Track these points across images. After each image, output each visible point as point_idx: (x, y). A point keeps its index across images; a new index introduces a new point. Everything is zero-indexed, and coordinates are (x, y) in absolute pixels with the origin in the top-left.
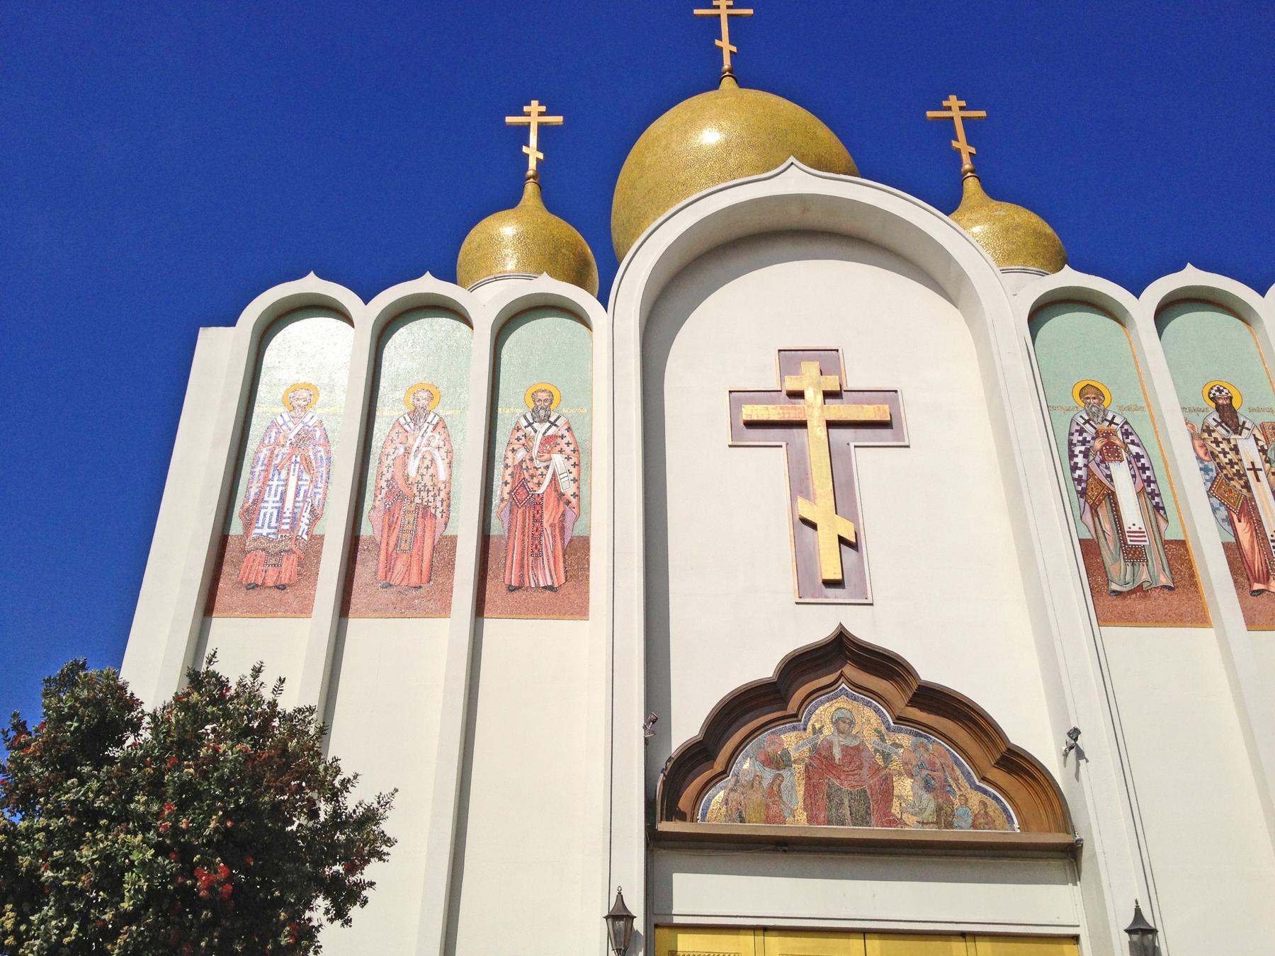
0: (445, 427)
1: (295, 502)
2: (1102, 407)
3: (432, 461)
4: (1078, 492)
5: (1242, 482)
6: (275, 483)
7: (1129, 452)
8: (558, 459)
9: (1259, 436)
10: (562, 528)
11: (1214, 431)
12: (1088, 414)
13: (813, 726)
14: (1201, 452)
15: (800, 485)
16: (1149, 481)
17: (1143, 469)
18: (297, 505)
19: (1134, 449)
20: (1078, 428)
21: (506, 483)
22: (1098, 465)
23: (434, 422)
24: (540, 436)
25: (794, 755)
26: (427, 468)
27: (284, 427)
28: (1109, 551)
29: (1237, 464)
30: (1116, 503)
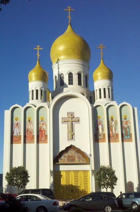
8: (44, 126)
17: (102, 126)
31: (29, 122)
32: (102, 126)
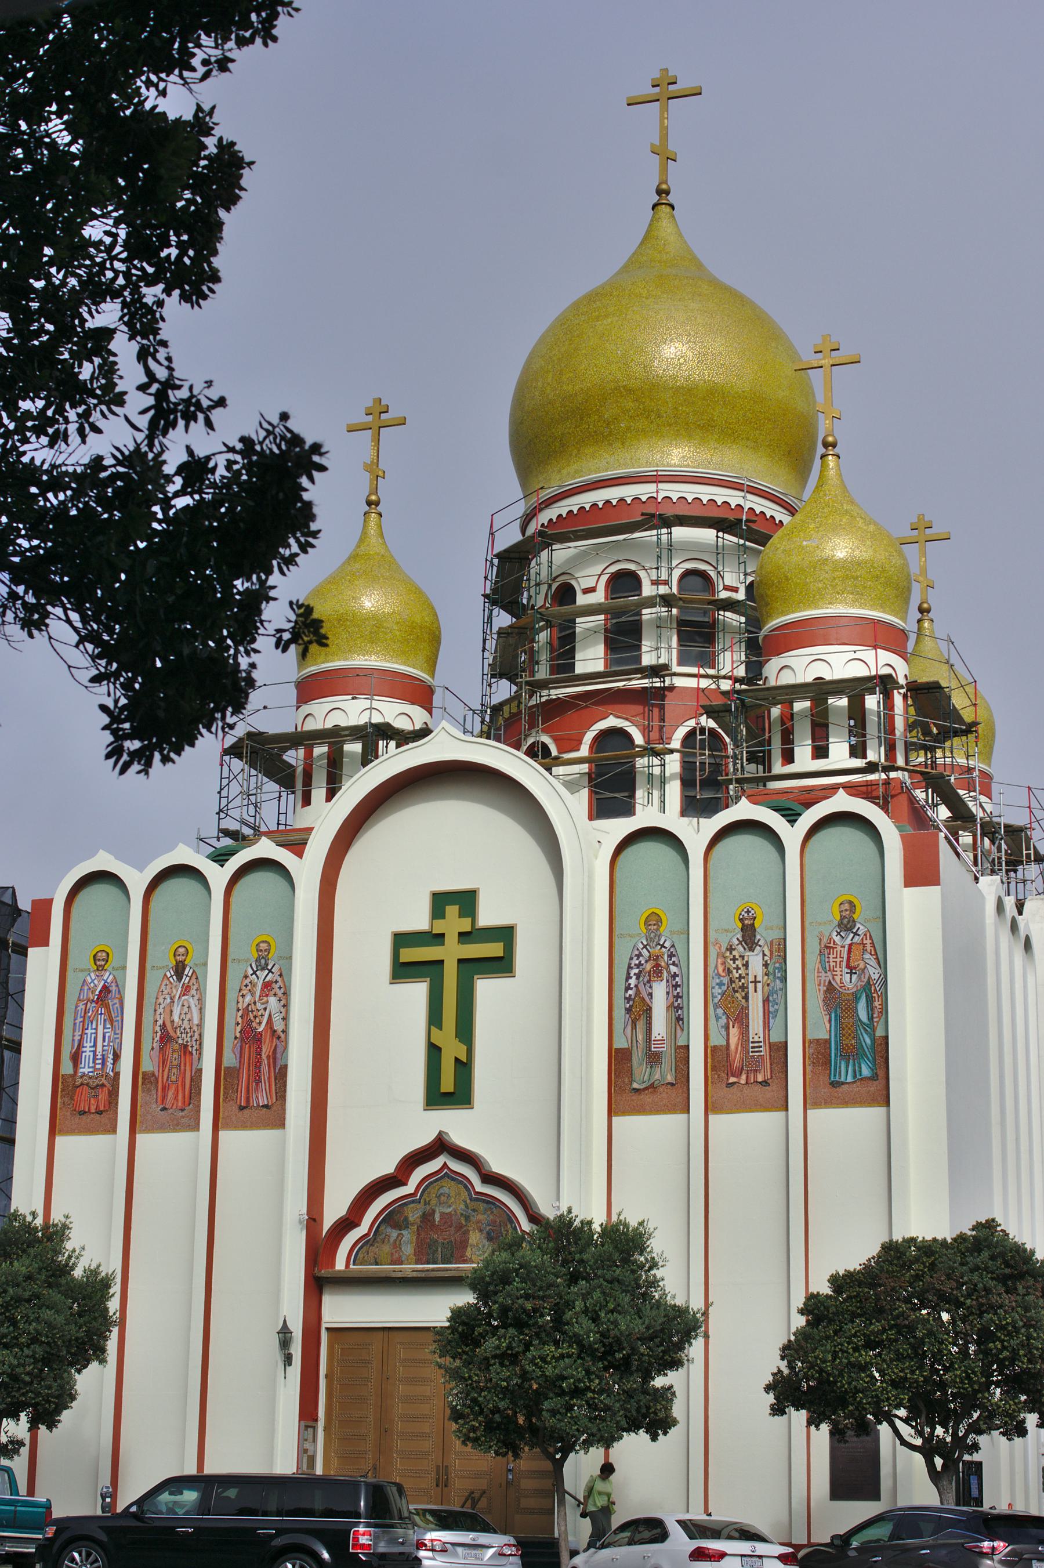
0: (197, 978)
1: (104, 1046)
2: (658, 933)
3: (189, 1007)
4: (626, 1009)
5: (743, 994)
6: (89, 1031)
7: (669, 972)
8: (272, 1000)
9: (767, 952)
10: (275, 1059)
11: (734, 949)
12: (647, 940)
13: (425, 1201)
14: (721, 969)
15: (435, 1018)
16: (678, 997)
18: (105, 1048)
19: (673, 969)
20: (637, 953)
21: (238, 1024)
22: (645, 985)
23: (190, 975)
24: (261, 982)
25: (411, 1219)
26: (186, 1014)
27: (92, 985)
28: (638, 1057)
29: (744, 978)
30: (650, 1017)
31: (180, 979)
32: (676, 986)
